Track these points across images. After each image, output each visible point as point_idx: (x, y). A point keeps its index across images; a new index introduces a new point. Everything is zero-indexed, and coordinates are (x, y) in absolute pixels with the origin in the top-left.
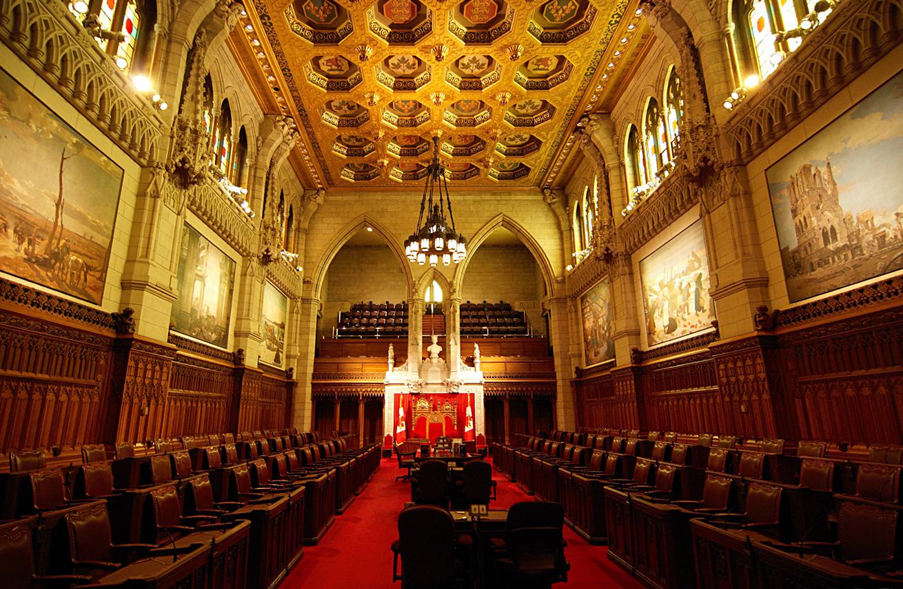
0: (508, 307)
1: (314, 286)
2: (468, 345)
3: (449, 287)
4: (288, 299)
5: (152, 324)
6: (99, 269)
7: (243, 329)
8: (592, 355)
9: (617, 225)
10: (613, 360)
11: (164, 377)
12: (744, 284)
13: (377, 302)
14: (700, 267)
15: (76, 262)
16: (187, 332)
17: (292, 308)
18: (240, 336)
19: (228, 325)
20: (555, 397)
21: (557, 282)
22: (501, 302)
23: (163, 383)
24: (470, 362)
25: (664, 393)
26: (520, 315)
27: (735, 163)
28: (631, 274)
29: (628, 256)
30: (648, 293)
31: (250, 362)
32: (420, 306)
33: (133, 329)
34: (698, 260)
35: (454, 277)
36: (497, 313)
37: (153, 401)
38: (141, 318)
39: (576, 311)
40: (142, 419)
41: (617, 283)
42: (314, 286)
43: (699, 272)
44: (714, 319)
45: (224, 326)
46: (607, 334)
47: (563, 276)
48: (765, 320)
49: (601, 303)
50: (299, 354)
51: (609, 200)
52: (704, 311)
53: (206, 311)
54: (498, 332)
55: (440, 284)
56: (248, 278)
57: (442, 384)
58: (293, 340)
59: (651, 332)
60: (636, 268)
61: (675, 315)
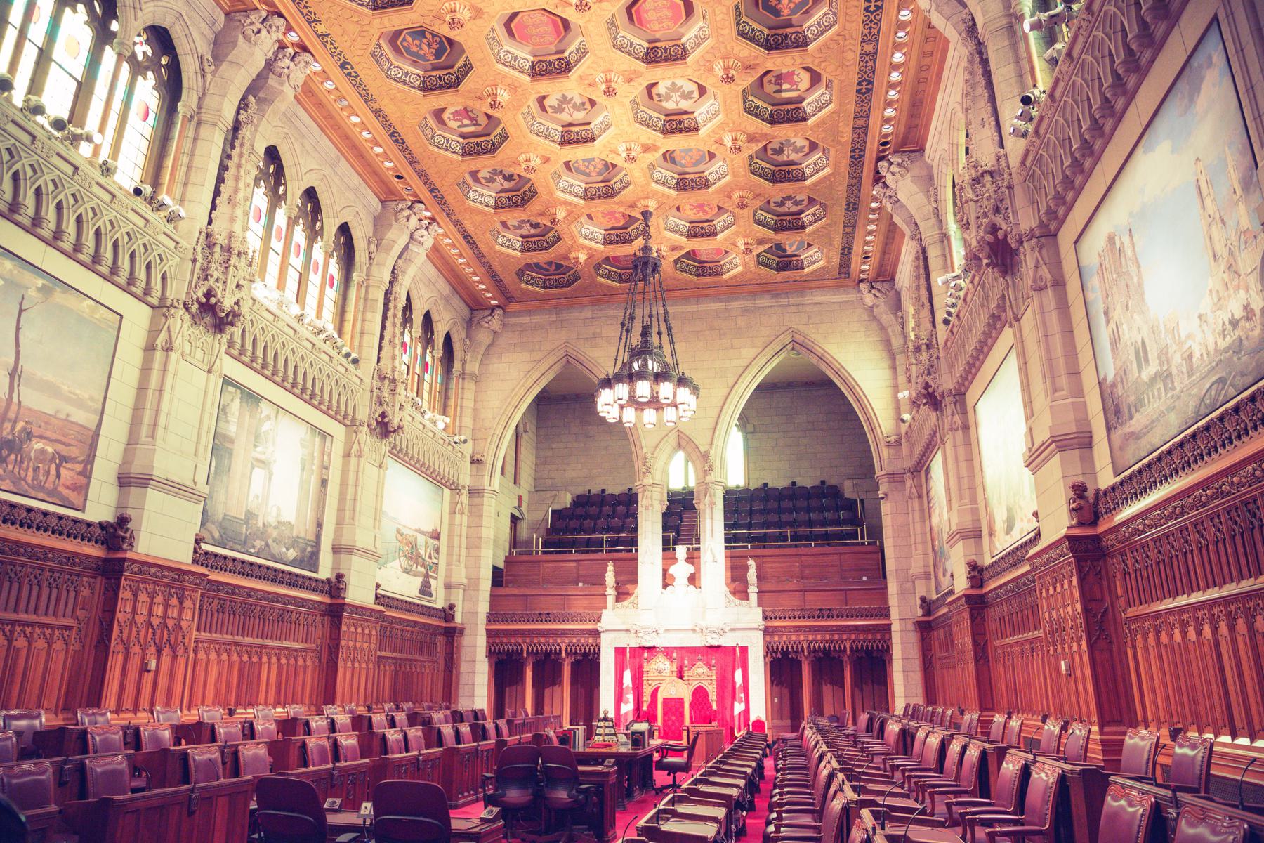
0: (835, 492)
1: (488, 468)
2: (738, 562)
4: (447, 492)
5: (164, 536)
6: (81, 459)
7: (345, 542)
8: (940, 575)
15: (43, 451)
16: (239, 547)
17: (453, 505)
19: (318, 537)
20: (887, 650)
21: (889, 445)
22: (823, 482)
26: (851, 505)
27: (1037, 233)
28: (966, 427)
29: (960, 396)
32: (656, 496)
33: (131, 545)
38: (143, 529)
39: (920, 497)
42: (488, 468)
45: (313, 538)
47: (899, 434)
50: (465, 581)
53: (274, 513)
54: (807, 538)
56: (353, 460)
58: (455, 557)
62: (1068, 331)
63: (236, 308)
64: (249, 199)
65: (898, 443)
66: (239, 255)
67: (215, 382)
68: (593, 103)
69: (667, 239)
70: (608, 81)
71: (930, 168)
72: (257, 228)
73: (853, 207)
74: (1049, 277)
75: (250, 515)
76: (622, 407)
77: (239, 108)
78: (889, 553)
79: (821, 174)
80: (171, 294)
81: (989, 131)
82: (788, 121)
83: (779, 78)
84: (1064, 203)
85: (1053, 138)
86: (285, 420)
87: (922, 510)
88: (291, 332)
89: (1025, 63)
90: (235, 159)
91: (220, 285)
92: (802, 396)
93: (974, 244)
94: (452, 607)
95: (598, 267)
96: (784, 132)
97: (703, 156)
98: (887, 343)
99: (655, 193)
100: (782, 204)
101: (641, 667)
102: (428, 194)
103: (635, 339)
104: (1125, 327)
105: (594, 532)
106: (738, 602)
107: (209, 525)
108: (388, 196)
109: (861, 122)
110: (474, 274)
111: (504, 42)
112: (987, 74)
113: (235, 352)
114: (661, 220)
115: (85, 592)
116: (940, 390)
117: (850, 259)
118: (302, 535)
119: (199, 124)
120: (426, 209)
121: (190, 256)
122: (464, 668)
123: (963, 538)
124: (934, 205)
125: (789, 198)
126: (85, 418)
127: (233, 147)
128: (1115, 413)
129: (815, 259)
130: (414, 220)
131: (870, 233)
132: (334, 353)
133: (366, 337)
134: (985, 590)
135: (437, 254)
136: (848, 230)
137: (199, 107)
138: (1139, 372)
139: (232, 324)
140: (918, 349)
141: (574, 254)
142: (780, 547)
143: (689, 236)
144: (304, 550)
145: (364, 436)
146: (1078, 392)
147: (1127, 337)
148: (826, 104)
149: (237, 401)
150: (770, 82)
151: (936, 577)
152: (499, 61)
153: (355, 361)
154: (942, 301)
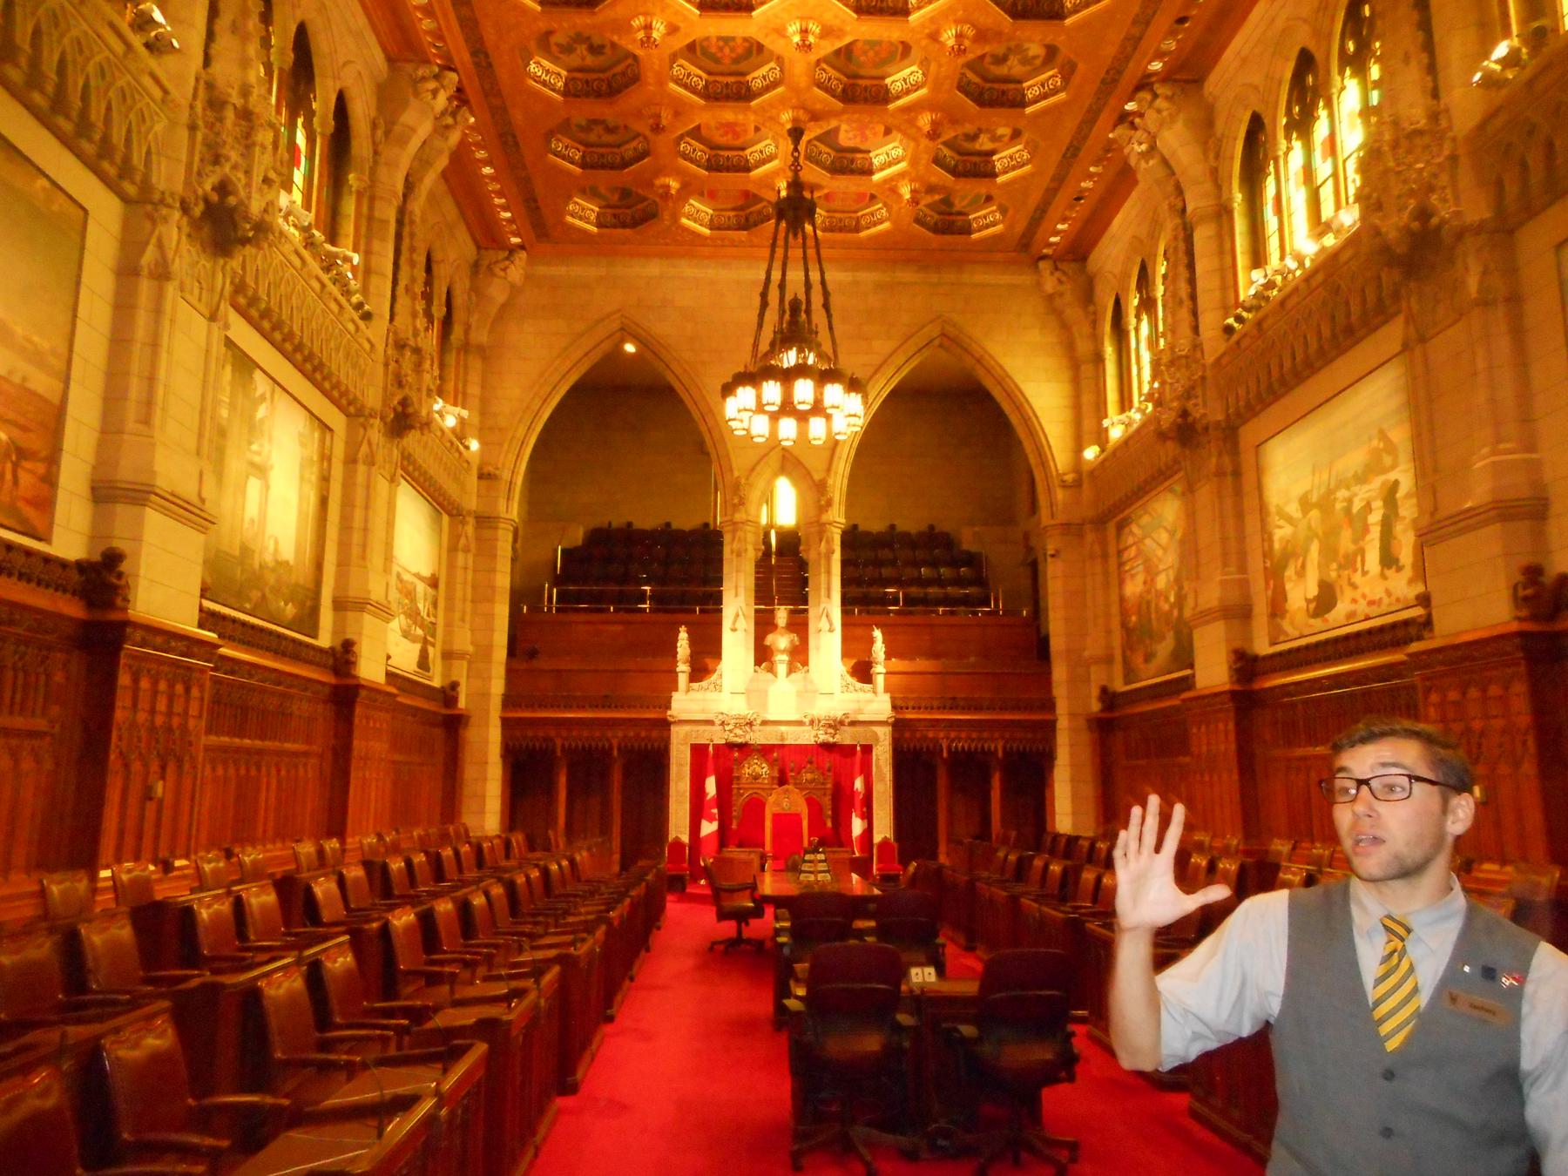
1: (504, 487)
2: (859, 631)
3: (815, 491)
4: (446, 518)
6: (44, 454)
7: (353, 592)
8: (1138, 660)
9: (1209, 359)
10: (1188, 672)
12: (1492, 513)
13: (647, 519)
14: (1394, 467)
16: (232, 601)
17: (455, 538)
18: (346, 610)
21: (1064, 485)
22: (932, 527)
24: (863, 672)
25: (1300, 752)
26: (972, 560)
28: (1237, 473)
29: (1230, 433)
30: (1275, 519)
32: (750, 538)
34: (1391, 448)
35: (829, 470)
36: (920, 554)
38: (142, 572)
39: (1105, 556)
41: (1205, 493)
42: (504, 487)
43: (1392, 476)
44: (1420, 588)
45: (311, 585)
46: (1176, 613)
48: (1535, 597)
49: (1164, 537)
50: (471, 649)
51: (1193, 297)
52: (1399, 569)
55: (795, 483)
56: (361, 468)
58: (457, 615)
59: (1277, 607)
60: (1247, 459)
61: (1333, 574)
65: (1077, 484)
75: (246, 551)
76: (775, 417)
79: (1052, 100)
86: (282, 401)
87: (1106, 573)
91: (241, 175)
92: (952, 411)
94: (454, 686)
98: (1070, 347)
101: (731, 771)
102: (466, 57)
103: (771, 316)
106: (859, 685)
110: (500, 194)
115: (59, 678)
116: (1204, 422)
118: (301, 582)
122: (469, 772)
124: (1212, 163)
126: (43, 383)
132: (343, 300)
133: (374, 280)
134: (1257, 686)
144: (302, 604)
145: (376, 433)
151: (1126, 663)
153: (367, 316)
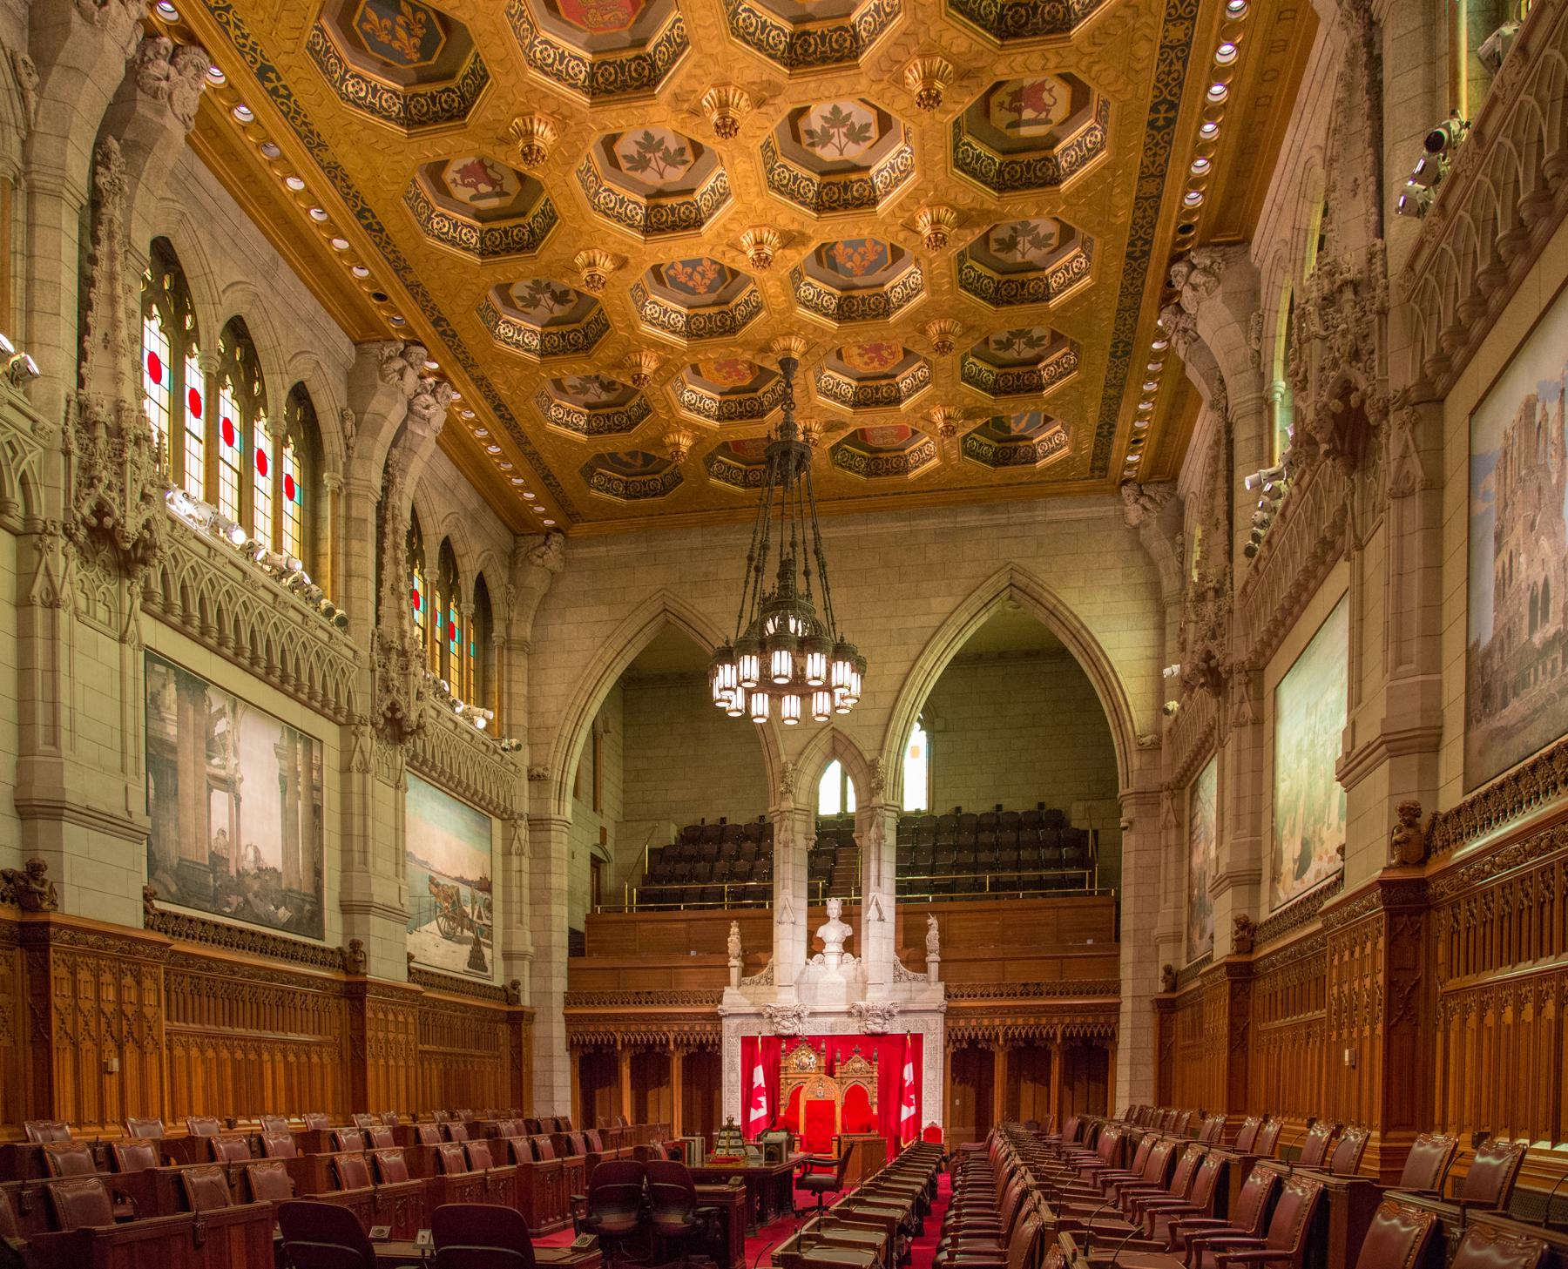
7: (357, 896)
11: (150, 999)
19: (318, 889)
23: (148, 1012)
31: (384, 968)
32: (799, 827)
37: (130, 1048)
40: (111, 1083)
45: (308, 889)
50: (531, 950)
57: (849, 1014)
62: (1434, 568)
63: (146, 534)
64: (138, 339)
66: (137, 442)
67: (135, 661)
68: (698, 149)
69: (822, 405)
70: (723, 105)
71: (1256, 275)
72: (157, 394)
73: (1124, 349)
74: (1420, 473)
75: (217, 860)
77: (95, 164)
78: (1127, 906)
80: (41, 512)
81: (1362, 205)
82: (1028, 185)
83: (1019, 97)
84: (1465, 343)
85: (1468, 218)
88: (238, 576)
89: (1444, 64)
90: (104, 265)
93: (1310, 416)
95: (710, 460)
96: (1024, 207)
97: (882, 254)
99: (803, 324)
100: (1006, 345)
104: (1523, 559)
105: (710, 880)
106: (911, 974)
107: (159, 873)
108: (365, 334)
109: (1150, 188)
111: (540, 24)
112: (1376, 89)
113: (157, 609)
114: (811, 375)
117: (1110, 444)
118: (295, 887)
119: (31, 194)
120: (431, 359)
121: (59, 444)
123: (1234, 884)
125: (1020, 334)
127: (96, 241)
128: (1484, 693)
129: (1055, 444)
130: (411, 378)
131: (1146, 397)
135: (453, 439)
136: (1112, 392)
137: (27, 161)
138: (1531, 632)
139: (145, 562)
140: (1201, 597)
141: (672, 438)
142: (974, 898)
143: (857, 404)
144: (300, 909)
146: (1433, 664)
147: (1523, 575)
148: (1094, 151)
149: (172, 687)
150: (1001, 105)
151: (1189, 939)
152: (532, 63)
154: (1251, 514)
